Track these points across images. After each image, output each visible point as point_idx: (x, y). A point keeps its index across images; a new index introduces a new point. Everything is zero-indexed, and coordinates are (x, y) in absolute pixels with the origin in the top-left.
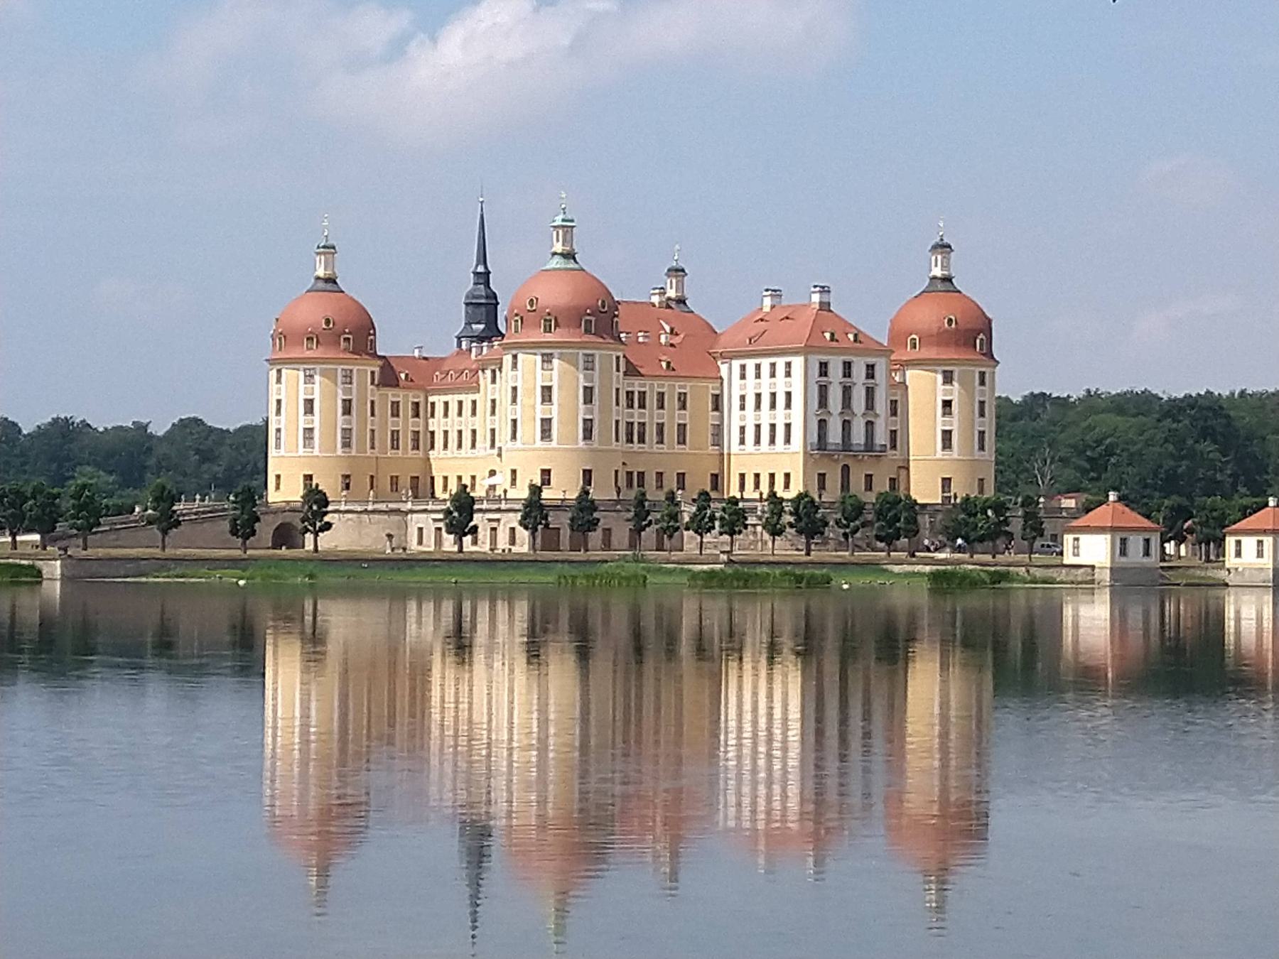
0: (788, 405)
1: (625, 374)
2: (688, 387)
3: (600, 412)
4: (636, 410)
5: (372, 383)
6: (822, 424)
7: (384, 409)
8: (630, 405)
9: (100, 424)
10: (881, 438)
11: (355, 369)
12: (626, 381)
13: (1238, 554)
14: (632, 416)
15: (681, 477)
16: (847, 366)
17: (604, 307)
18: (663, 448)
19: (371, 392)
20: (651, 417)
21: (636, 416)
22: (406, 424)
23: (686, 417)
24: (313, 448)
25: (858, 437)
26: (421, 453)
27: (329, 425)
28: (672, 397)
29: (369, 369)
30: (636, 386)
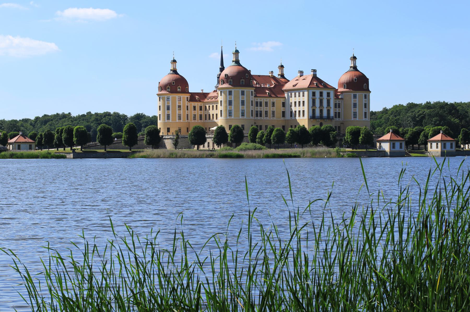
0: (303, 105)
1: (255, 96)
2: (275, 100)
4: (259, 107)
5: (187, 101)
6: (314, 111)
7: (191, 108)
8: (257, 106)
9: (50, 114)
10: (332, 114)
11: (182, 96)
12: (255, 99)
13: (431, 147)
14: (257, 109)
15: (266, 127)
16: (321, 94)
19: (187, 103)
20: (264, 108)
21: (259, 109)
22: (198, 112)
25: (325, 114)
26: (202, 121)
27: (174, 112)
29: (186, 96)
30: (259, 100)
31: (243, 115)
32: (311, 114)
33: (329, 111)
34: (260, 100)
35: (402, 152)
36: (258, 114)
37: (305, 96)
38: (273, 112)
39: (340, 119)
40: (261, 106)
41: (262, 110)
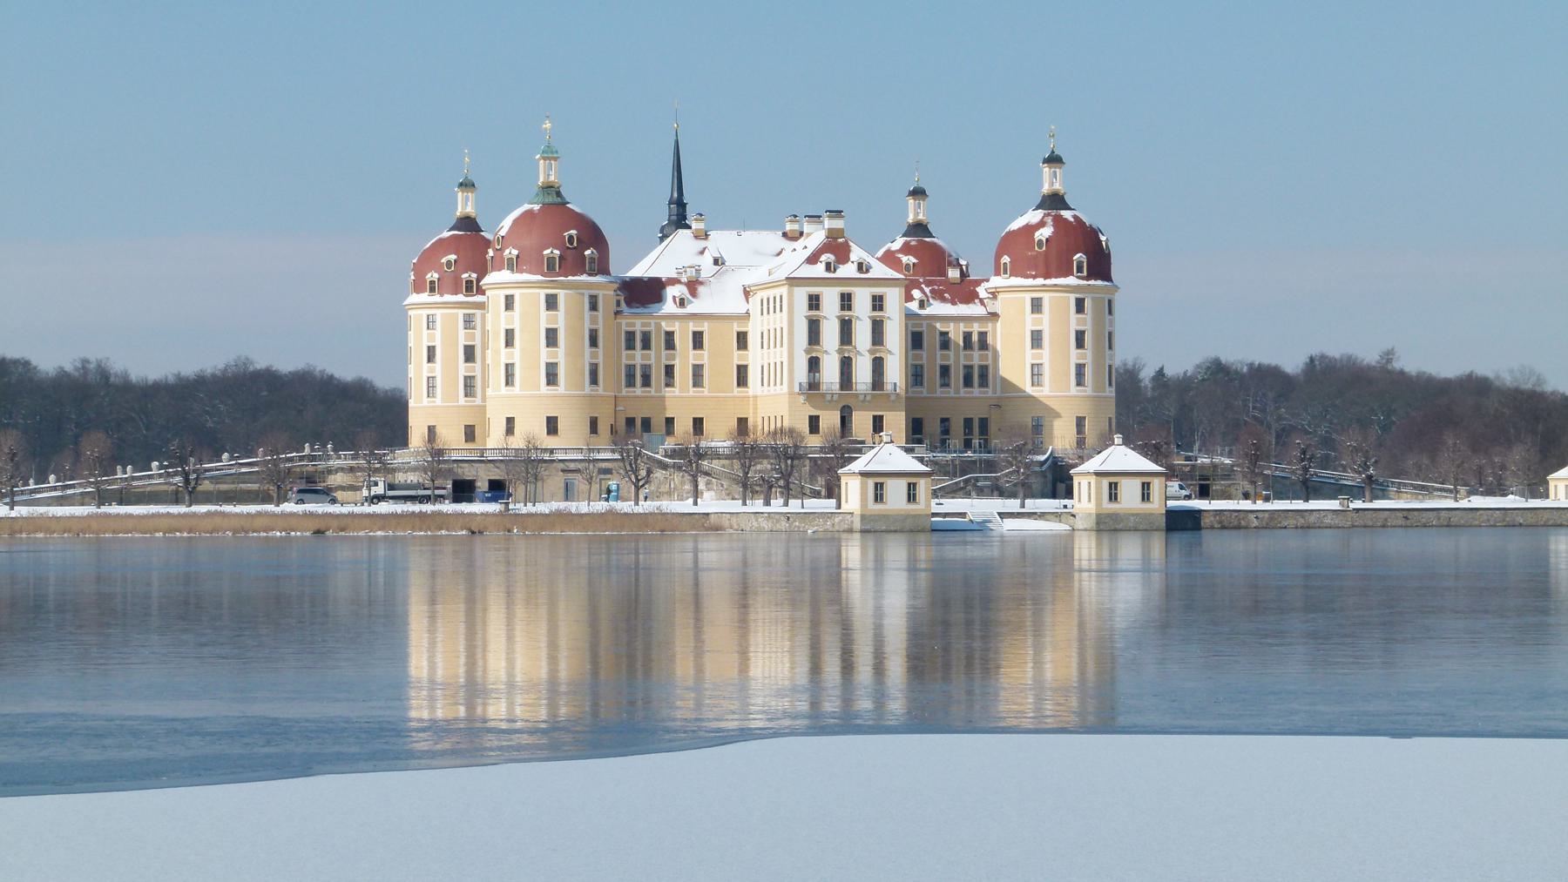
3: (567, 355)
6: (814, 364)
8: (630, 345)
14: (633, 357)
16: (846, 301)
17: (572, 244)
18: (674, 392)
20: (658, 358)
21: (638, 357)
23: (704, 357)
25: (862, 374)
28: (658, 335)
31: (552, 378)
32: (802, 374)
33: (878, 365)
34: (643, 325)
35: (915, 516)
36: (634, 376)
38: (698, 372)
39: (989, 392)
40: (646, 345)
41: (652, 361)
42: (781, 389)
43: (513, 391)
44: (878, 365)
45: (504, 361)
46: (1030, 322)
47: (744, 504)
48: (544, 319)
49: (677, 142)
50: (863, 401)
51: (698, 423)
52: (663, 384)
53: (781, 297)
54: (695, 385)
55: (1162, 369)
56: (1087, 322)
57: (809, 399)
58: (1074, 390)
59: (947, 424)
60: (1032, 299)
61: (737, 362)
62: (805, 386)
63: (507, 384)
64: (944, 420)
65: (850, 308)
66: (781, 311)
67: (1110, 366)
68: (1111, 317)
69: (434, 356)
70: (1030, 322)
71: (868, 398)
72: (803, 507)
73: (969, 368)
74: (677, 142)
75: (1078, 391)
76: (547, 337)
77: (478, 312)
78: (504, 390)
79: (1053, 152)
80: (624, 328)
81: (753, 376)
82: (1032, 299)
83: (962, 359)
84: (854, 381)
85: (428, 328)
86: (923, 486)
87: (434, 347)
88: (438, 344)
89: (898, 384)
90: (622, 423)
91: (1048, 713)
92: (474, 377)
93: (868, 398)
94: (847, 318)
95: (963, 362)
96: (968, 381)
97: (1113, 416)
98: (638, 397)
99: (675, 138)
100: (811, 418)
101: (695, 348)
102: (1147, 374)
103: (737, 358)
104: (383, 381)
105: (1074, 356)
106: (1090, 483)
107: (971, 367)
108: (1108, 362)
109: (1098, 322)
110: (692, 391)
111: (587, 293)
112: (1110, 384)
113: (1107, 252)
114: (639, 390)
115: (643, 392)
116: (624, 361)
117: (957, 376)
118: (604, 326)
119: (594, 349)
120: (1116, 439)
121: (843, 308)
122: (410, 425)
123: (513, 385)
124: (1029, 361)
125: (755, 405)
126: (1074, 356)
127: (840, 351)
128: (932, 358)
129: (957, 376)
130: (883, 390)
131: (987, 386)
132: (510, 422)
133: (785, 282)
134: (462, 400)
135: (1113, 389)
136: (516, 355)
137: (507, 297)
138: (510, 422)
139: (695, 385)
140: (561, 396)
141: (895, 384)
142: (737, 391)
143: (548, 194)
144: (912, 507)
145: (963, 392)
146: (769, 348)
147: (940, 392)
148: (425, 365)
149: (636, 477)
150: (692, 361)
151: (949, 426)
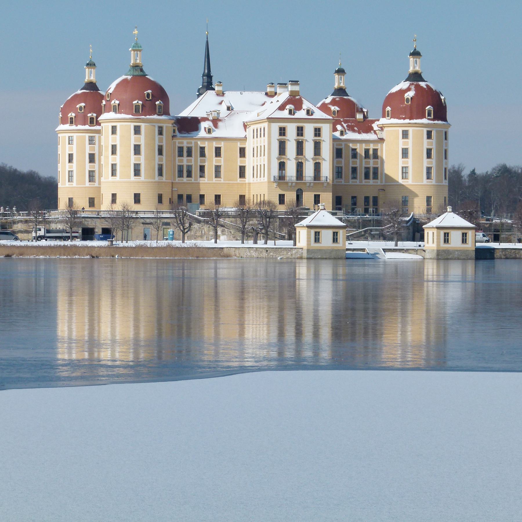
3: (146, 159)
6: (282, 166)
8: (181, 154)
14: (182, 161)
16: (300, 131)
21: (185, 161)
23: (221, 161)
24: (95, 182)
25: (309, 171)
31: (137, 172)
32: (275, 171)
33: (317, 167)
34: (188, 143)
35: (336, 250)
36: (183, 171)
37: (265, 135)
38: (218, 169)
40: (189, 154)
41: (193, 163)
42: (264, 180)
43: (116, 179)
44: (317, 167)
45: (111, 162)
46: (401, 144)
47: (243, 243)
48: (133, 139)
49: (207, 42)
50: (309, 186)
51: (218, 198)
52: (198, 176)
53: (264, 128)
54: (216, 177)
55: (474, 170)
56: (433, 144)
57: (279, 185)
58: (425, 181)
59: (355, 199)
60: (403, 131)
61: (239, 164)
62: (277, 178)
63: (112, 175)
64: (354, 198)
65: (302, 135)
66: (264, 136)
67: (445, 169)
68: (446, 141)
69: (72, 159)
70: (401, 144)
71: (312, 185)
72: (275, 245)
73: (367, 169)
74: (207, 42)
75: (427, 182)
76: (135, 150)
77: (97, 135)
78: (111, 179)
79: (415, 49)
80: (178, 145)
81: (248, 172)
82: (403, 131)
83: (364, 163)
84: (304, 175)
85: (69, 144)
86: (342, 234)
87: (72, 154)
88: (74, 152)
89: (328, 177)
90: (176, 197)
91: (409, 359)
92: (94, 171)
93: (312, 185)
94: (300, 140)
95: (364, 165)
96: (367, 176)
97: (447, 196)
98: (184, 183)
99: (206, 39)
100: (280, 195)
101: (216, 156)
102: (466, 173)
103: (239, 162)
104: (44, 173)
105: (426, 163)
106: (433, 233)
107: (368, 168)
108: (444, 166)
109: (439, 144)
110: (215, 180)
111: (157, 125)
112: (445, 179)
113: (444, 105)
114: (185, 179)
115: (187, 180)
116: (177, 163)
117: (361, 173)
118: (166, 144)
119: (160, 156)
120: (448, 209)
121: (298, 135)
122: (59, 197)
123: (115, 176)
124: (401, 165)
125: (249, 188)
126: (426, 163)
127: (296, 159)
128: (347, 163)
129: (361, 173)
130: (320, 181)
131: (377, 179)
132: (114, 196)
133: (266, 120)
134: (87, 184)
135: (447, 181)
136: (117, 159)
137: (113, 127)
138: (114, 196)
139: (216, 177)
140: (143, 182)
141: (327, 177)
142: (239, 180)
143: (136, 70)
144: (335, 245)
145: (364, 182)
146: (257, 156)
147: (351, 182)
148: (67, 164)
149: (183, 227)
150: (215, 164)
151: (356, 201)
